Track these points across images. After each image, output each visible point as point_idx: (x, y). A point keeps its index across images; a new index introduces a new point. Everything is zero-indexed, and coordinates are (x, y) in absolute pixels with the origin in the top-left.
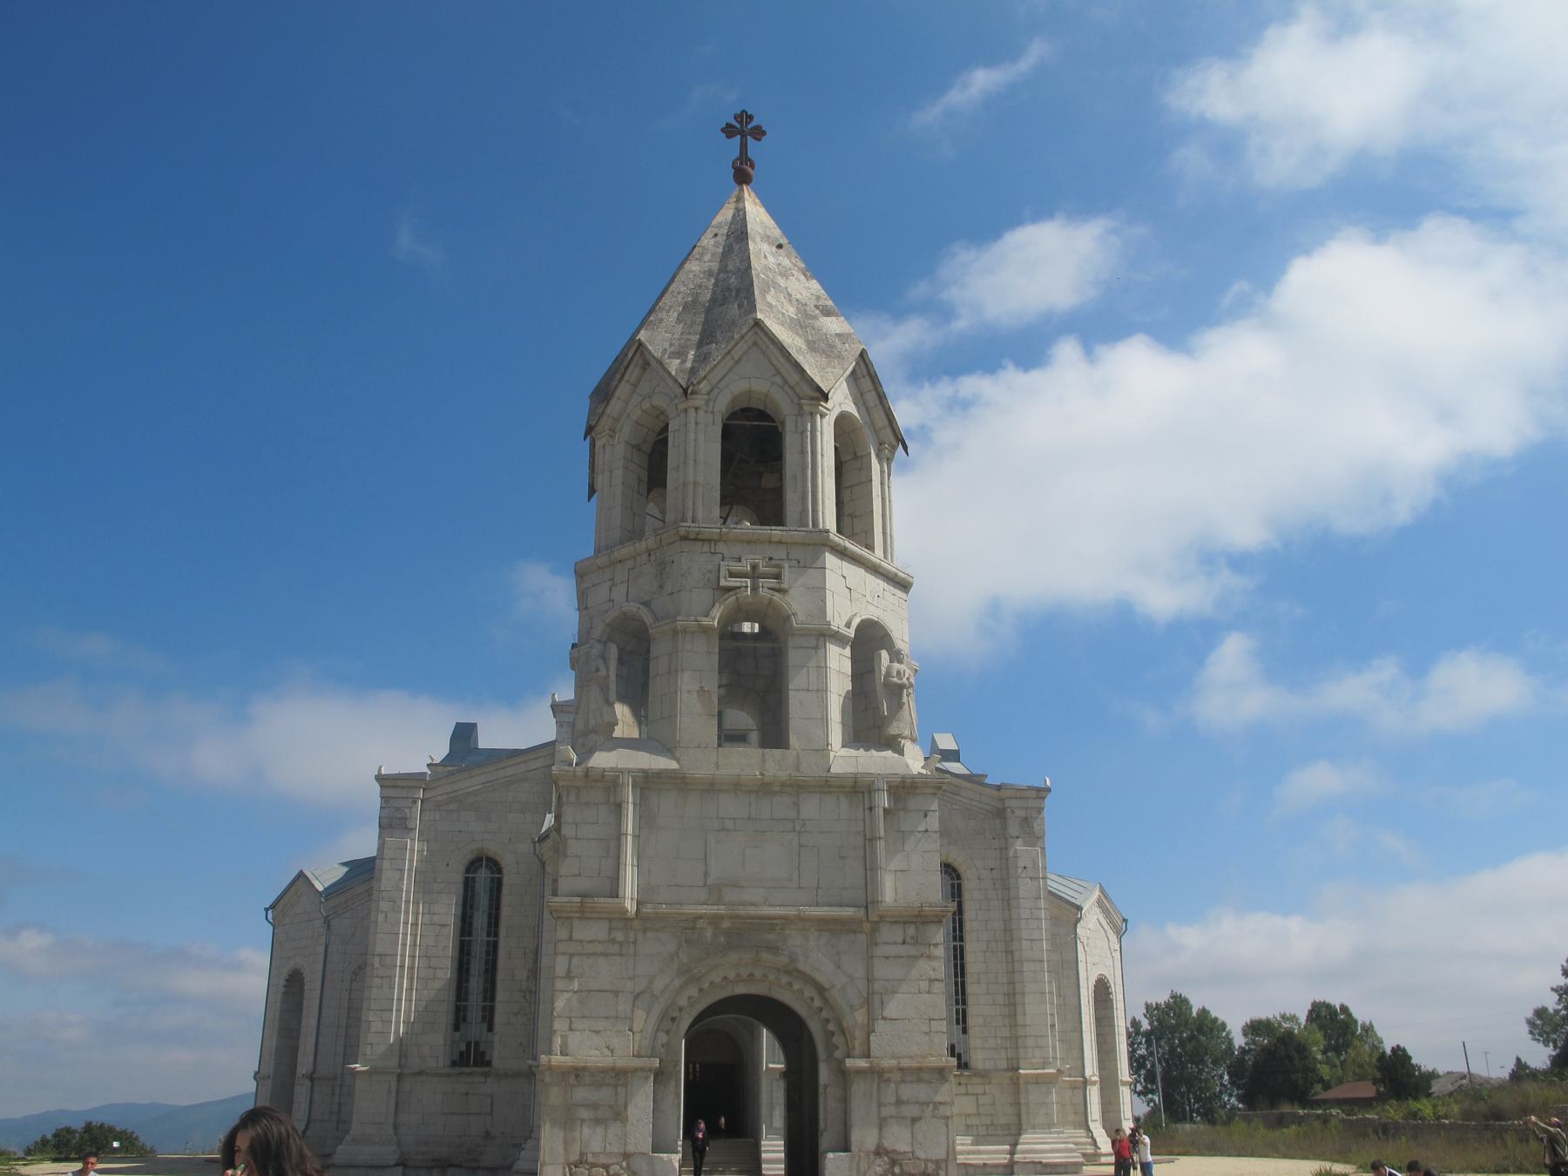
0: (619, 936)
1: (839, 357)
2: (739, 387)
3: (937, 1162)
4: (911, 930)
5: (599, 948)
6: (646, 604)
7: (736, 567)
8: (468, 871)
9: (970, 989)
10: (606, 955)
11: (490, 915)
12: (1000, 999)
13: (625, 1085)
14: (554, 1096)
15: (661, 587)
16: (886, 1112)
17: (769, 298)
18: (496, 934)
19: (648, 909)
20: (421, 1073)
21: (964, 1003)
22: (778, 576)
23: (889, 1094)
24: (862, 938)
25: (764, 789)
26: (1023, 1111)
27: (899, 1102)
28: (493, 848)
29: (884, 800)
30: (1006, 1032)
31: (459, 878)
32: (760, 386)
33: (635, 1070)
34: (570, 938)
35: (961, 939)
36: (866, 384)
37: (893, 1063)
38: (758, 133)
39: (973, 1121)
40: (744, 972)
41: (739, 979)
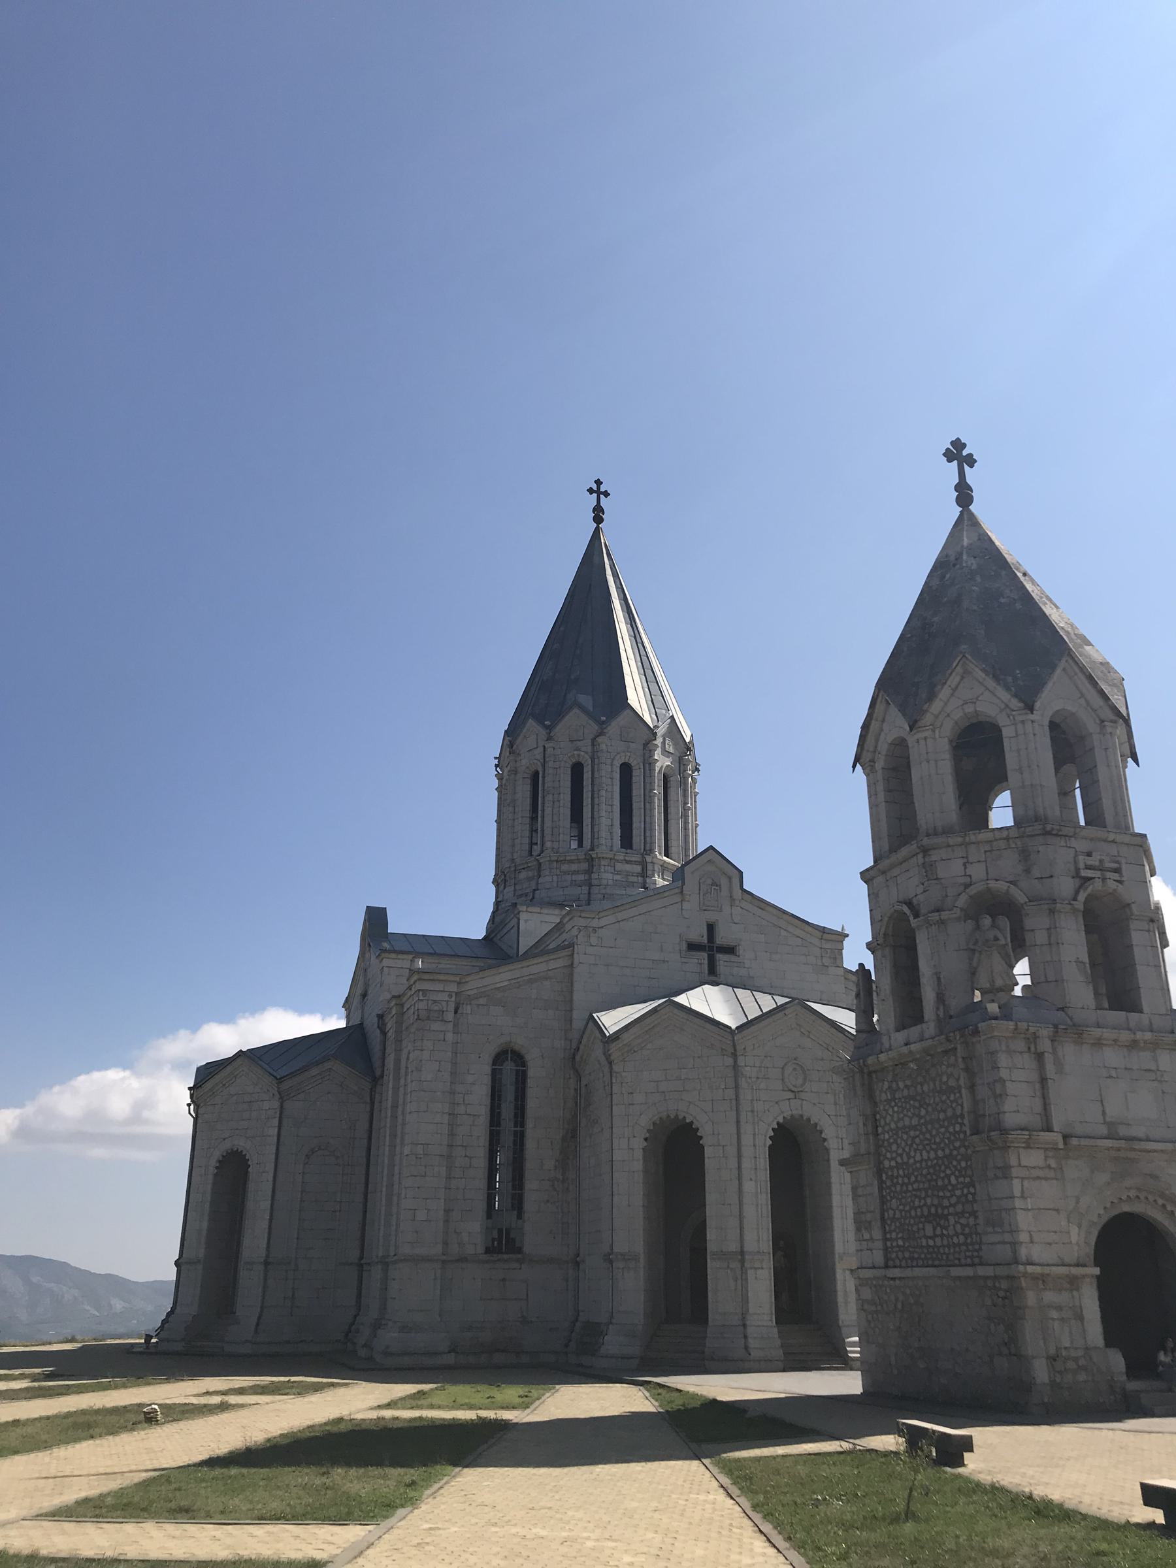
0: (1053, 1163)
2: (1057, 706)
5: (1040, 1173)
6: (1011, 882)
7: (1090, 861)
8: (494, 1064)
10: (1046, 1179)
11: (516, 1108)
13: (1077, 1290)
14: (1031, 1298)
15: (1027, 871)
18: (522, 1125)
20: (463, 1259)
22: (1117, 871)
28: (519, 1042)
31: (487, 1069)
33: (1084, 1276)
34: (1020, 1165)
40: (1132, 1194)
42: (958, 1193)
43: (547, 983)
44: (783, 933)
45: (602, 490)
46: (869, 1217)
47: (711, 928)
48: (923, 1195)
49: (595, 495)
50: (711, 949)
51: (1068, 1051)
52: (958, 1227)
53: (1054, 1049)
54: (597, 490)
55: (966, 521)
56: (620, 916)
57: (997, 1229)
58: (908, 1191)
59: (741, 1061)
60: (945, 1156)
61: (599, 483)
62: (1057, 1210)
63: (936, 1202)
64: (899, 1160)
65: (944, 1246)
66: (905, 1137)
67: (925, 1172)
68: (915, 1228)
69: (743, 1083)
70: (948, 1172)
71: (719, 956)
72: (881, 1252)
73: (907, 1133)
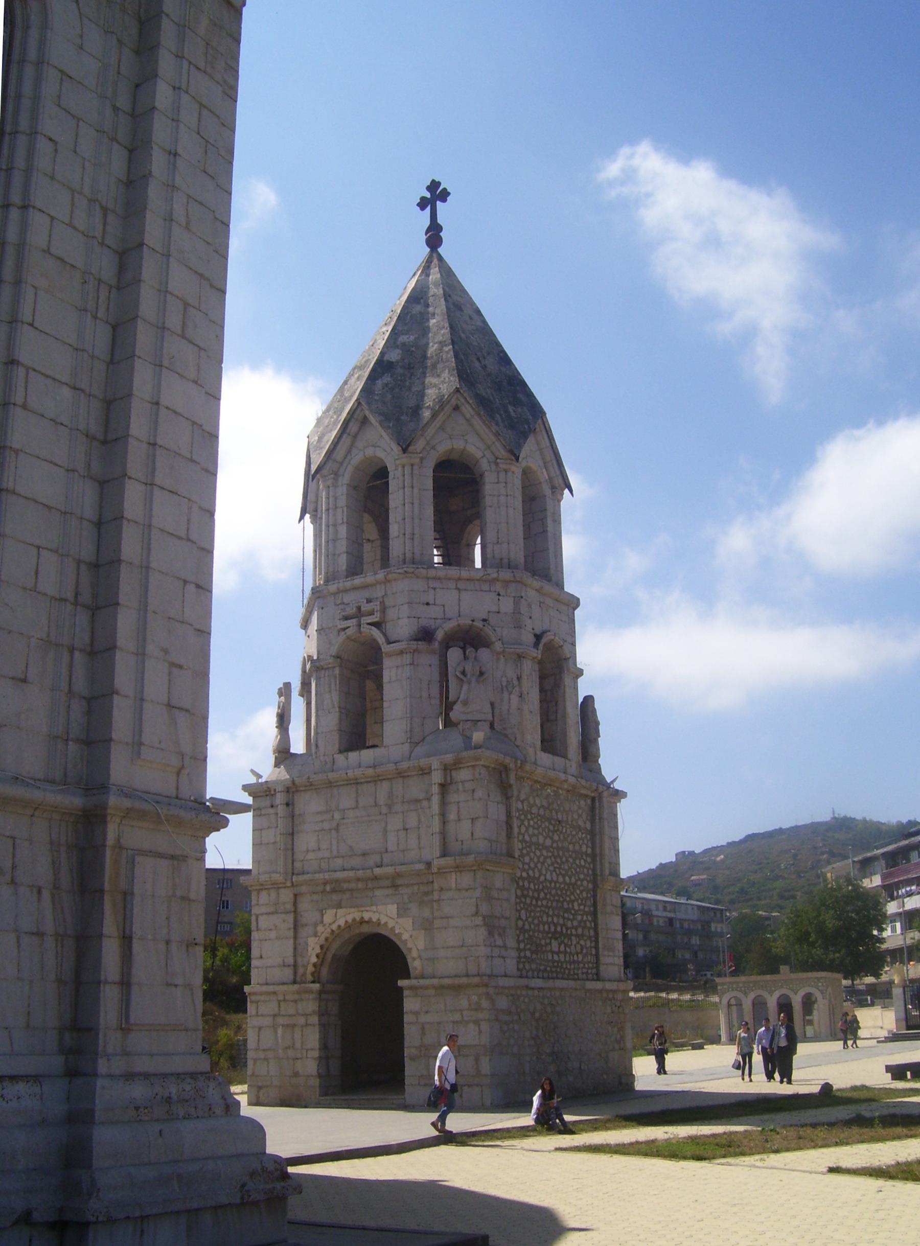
42: (579, 918)
46: (503, 922)
48: (551, 913)
52: (579, 947)
57: (611, 954)
58: (536, 906)
60: (571, 883)
63: (561, 921)
64: (531, 872)
65: (565, 961)
66: (538, 853)
67: (553, 892)
68: (543, 942)
70: (572, 897)
72: (515, 961)
73: (540, 850)
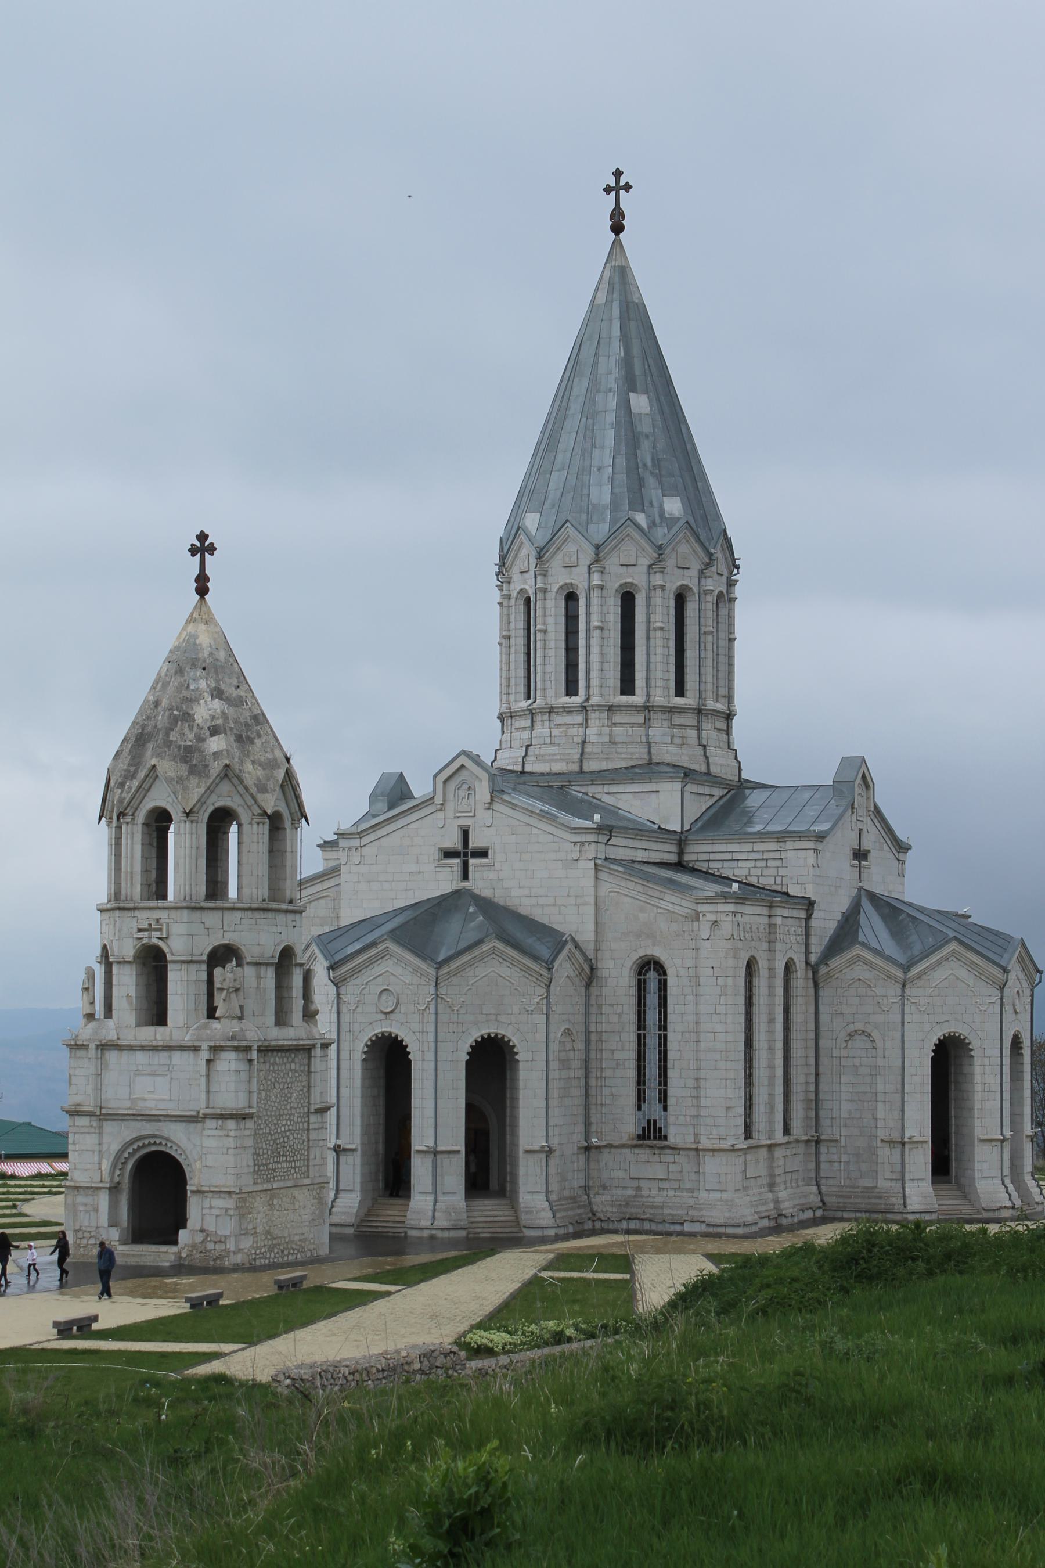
0: (94, 1124)
1: (208, 776)
3: (225, 1237)
4: (220, 1122)
5: (86, 1130)
9: (670, 1073)
12: (691, 1083)
16: (205, 1211)
17: (173, 736)
19: (103, 1111)
21: (666, 1084)
22: (160, 930)
23: (206, 1204)
24: (200, 1125)
25: (155, 1049)
26: (702, 1179)
27: (211, 1207)
29: (205, 1055)
30: (693, 1112)
32: (162, 804)
33: (101, 1188)
35: (665, 1029)
36: (235, 781)
37: (207, 1189)
38: (211, 549)
39: (662, 1185)
41: (150, 1144)
43: (322, 902)
44: (535, 831)
45: (622, 183)
47: (465, 834)
49: (613, 193)
50: (465, 855)
51: (112, 1056)
53: (102, 1053)
54: (618, 187)
55: (202, 614)
56: (380, 833)
59: (343, 990)
61: (618, 174)
62: (93, 1151)
69: (344, 1009)
71: (472, 861)
